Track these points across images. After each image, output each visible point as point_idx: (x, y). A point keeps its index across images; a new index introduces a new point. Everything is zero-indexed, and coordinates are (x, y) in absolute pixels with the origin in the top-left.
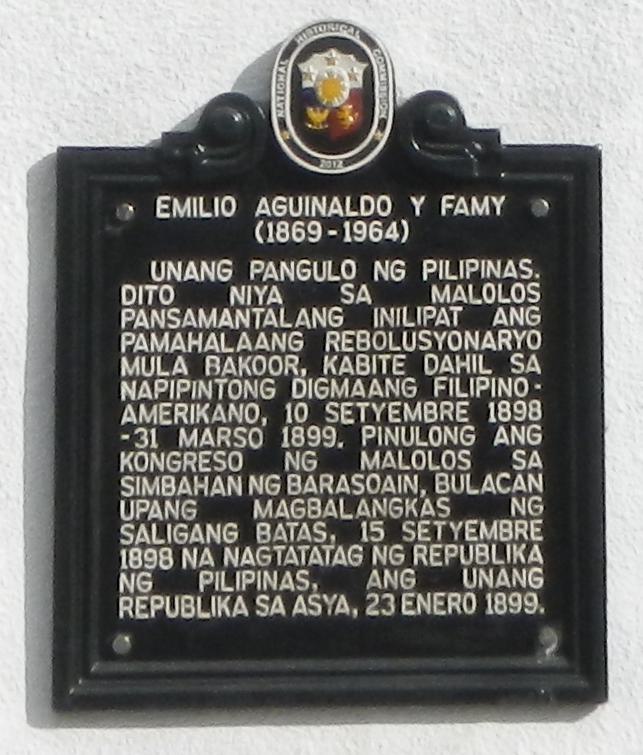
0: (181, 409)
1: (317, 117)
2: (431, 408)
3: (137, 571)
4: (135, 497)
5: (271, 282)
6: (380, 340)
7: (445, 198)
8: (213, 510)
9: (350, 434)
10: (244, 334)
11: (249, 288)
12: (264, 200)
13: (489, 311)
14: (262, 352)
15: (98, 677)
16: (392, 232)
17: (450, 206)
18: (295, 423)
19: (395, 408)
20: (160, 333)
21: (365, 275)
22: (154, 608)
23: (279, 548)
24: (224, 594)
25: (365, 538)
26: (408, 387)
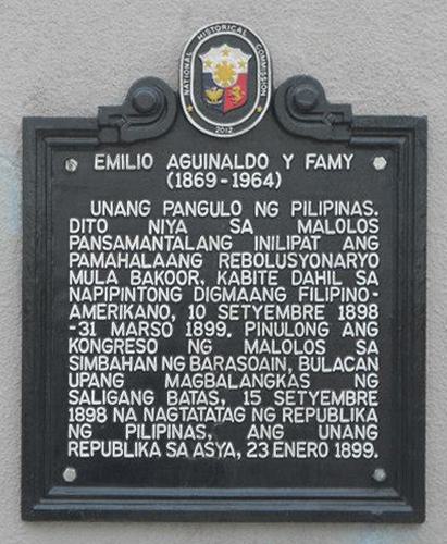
0: (113, 308)
1: (213, 95)
4: (79, 371)
5: (179, 216)
7: (308, 156)
8: (135, 381)
9: (236, 327)
10: (159, 256)
17: (313, 162)
20: (97, 253)
21: (248, 211)
23: (183, 409)
24: (144, 441)
25: (247, 403)
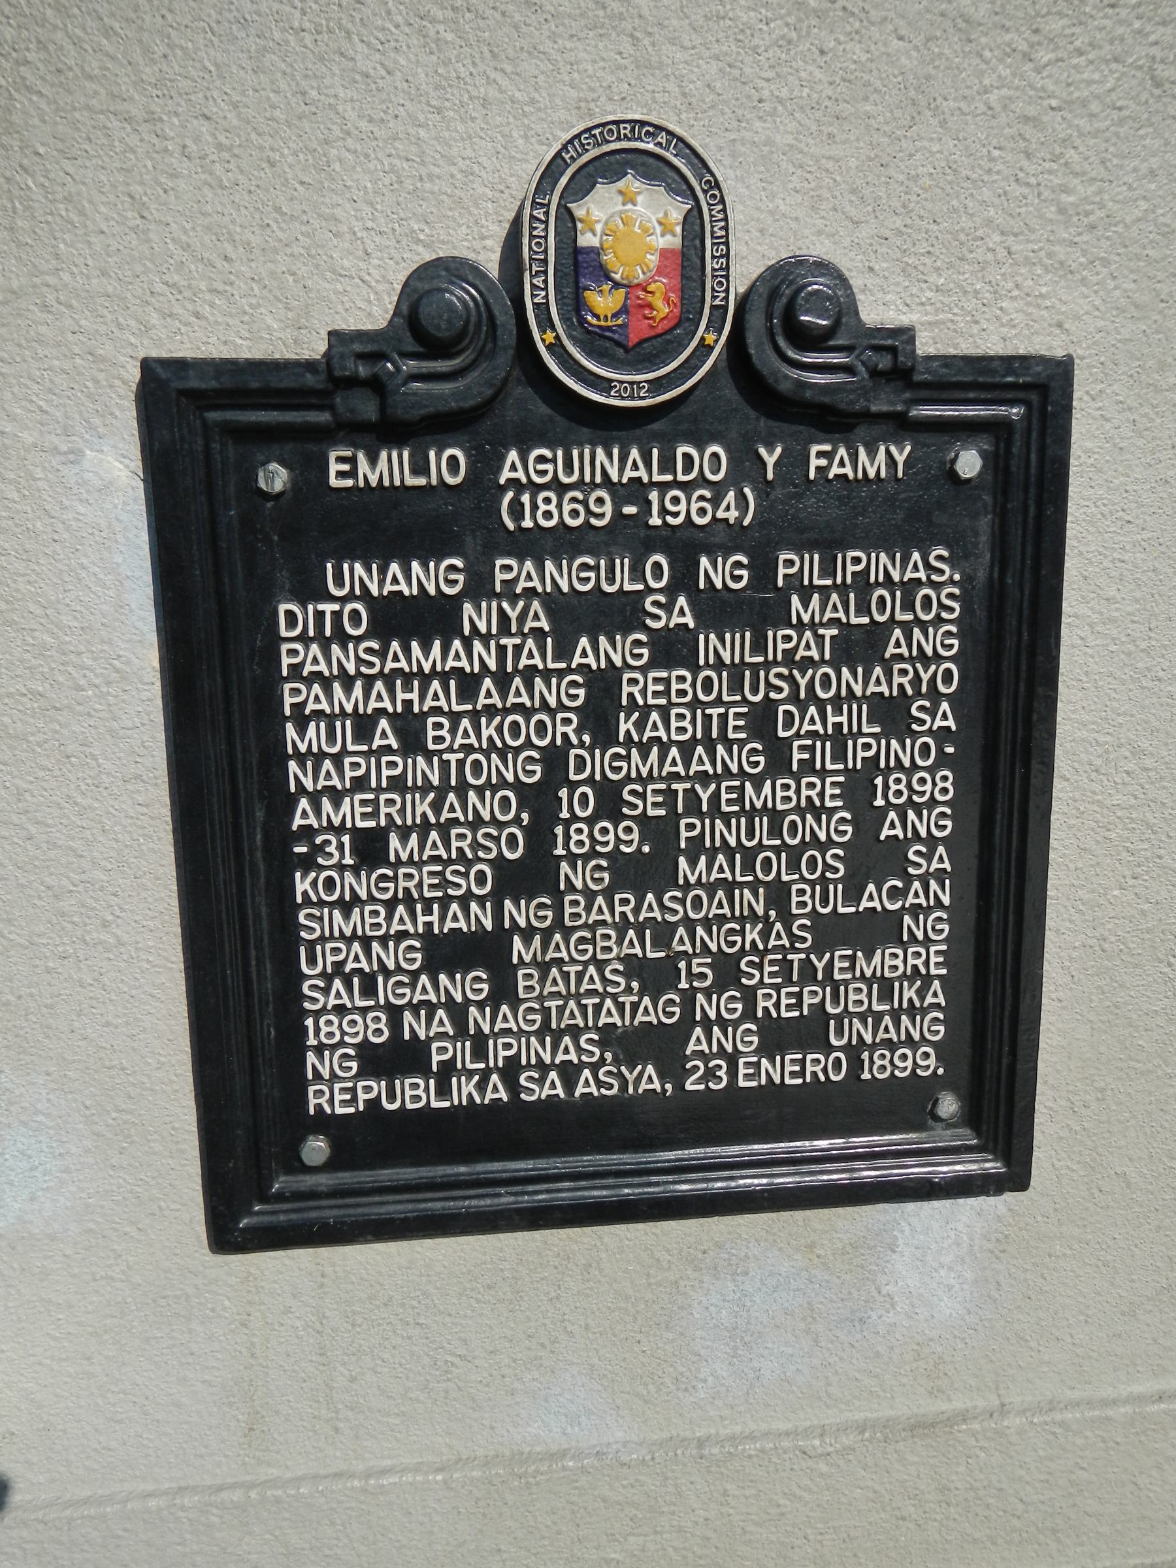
0: (390, 802)
1: (603, 302)
2: (786, 787)
3: (334, 1048)
4: (323, 939)
5: (530, 593)
6: (708, 685)
7: (815, 449)
8: (446, 954)
9: (660, 832)
10: (488, 683)
11: (494, 604)
12: (513, 456)
13: (876, 635)
14: (519, 708)
15: (280, 1197)
16: (728, 509)
17: (823, 462)
18: (575, 818)
19: (730, 789)
20: (348, 682)
21: (683, 579)
22: (362, 1096)
23: (553, 1004)
24: (471, 1073)
25: (683, 985)
26: (751, 757)
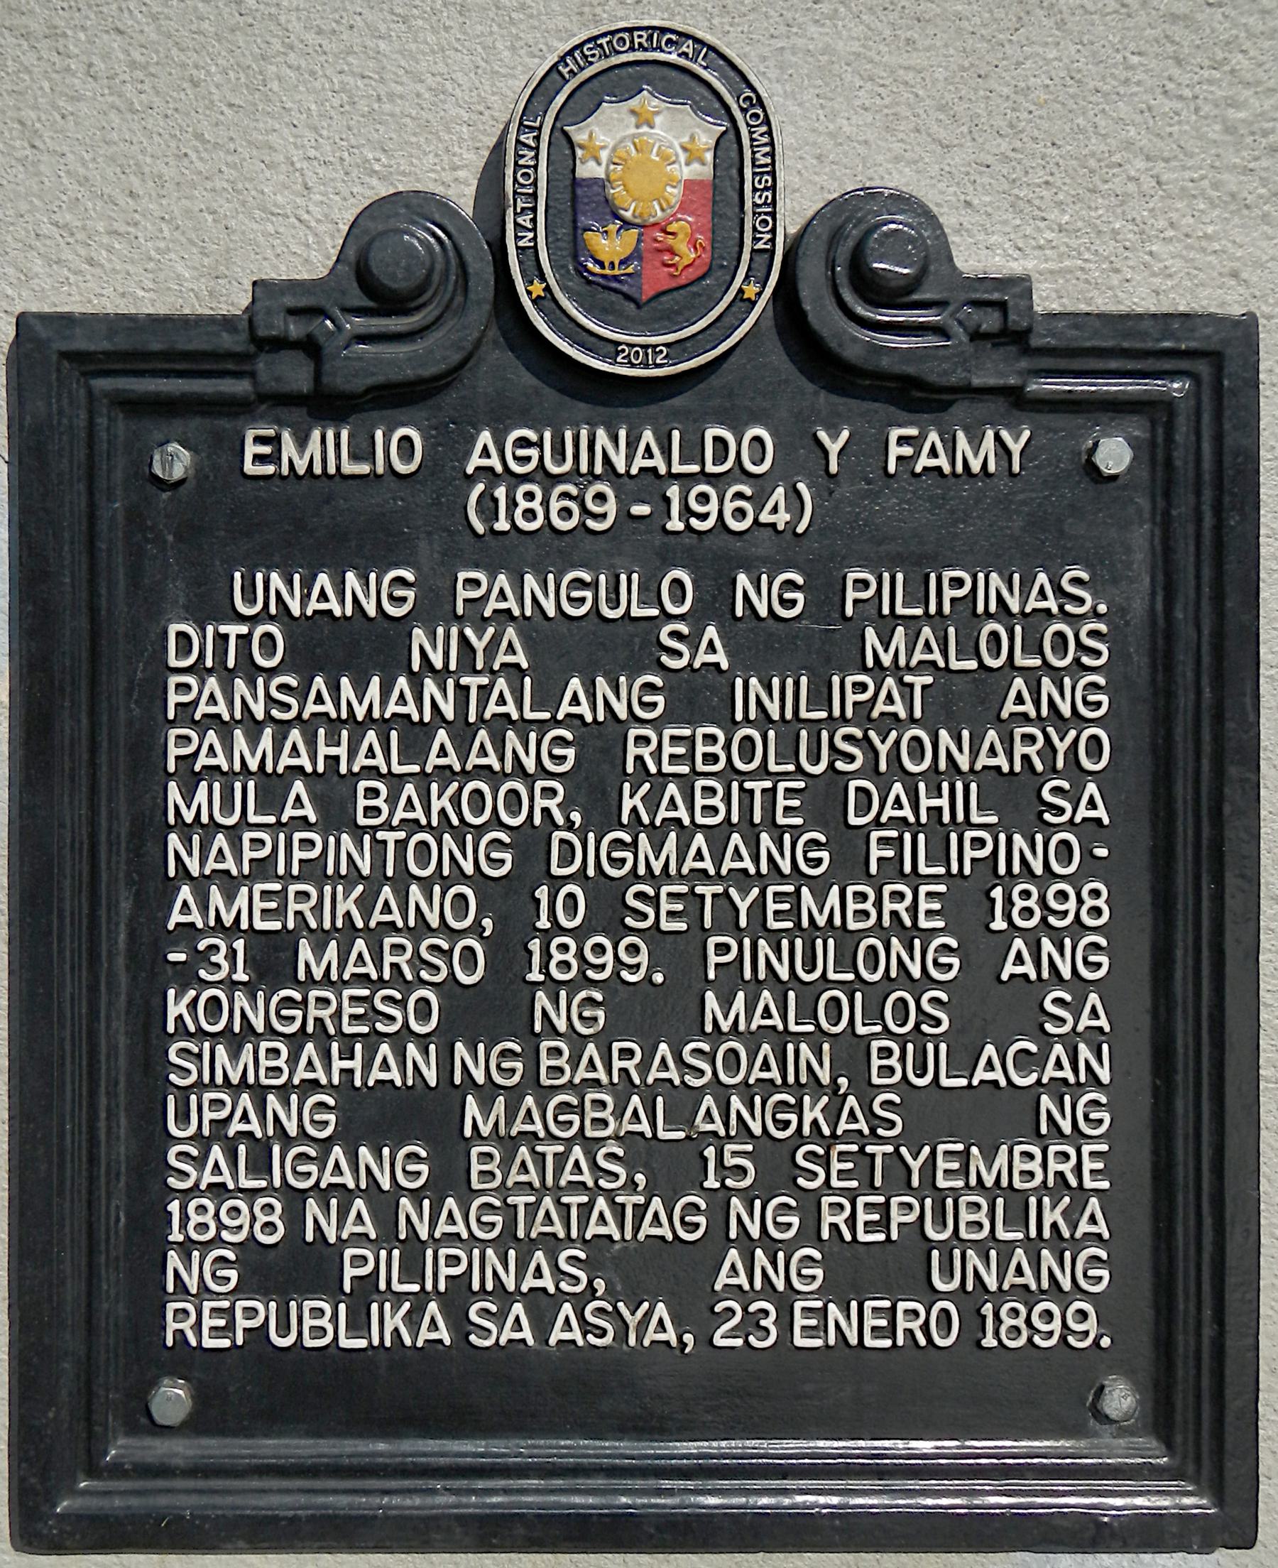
1: (609, 246)
2: (862, 897)
3: (206, 1246)
4: (199, 1086)
8: (372, 1116)
10: (442, 736)
11: (454, 631)
13: (989, 685)
16: (775, 510)
17: (907, 451)
18: (559, 929)
20: (254, 728)
21: (715, 603)
22: (242, 1323)
23: (520, 1200)
24: (400, 1297)
25: (712, 1183)
